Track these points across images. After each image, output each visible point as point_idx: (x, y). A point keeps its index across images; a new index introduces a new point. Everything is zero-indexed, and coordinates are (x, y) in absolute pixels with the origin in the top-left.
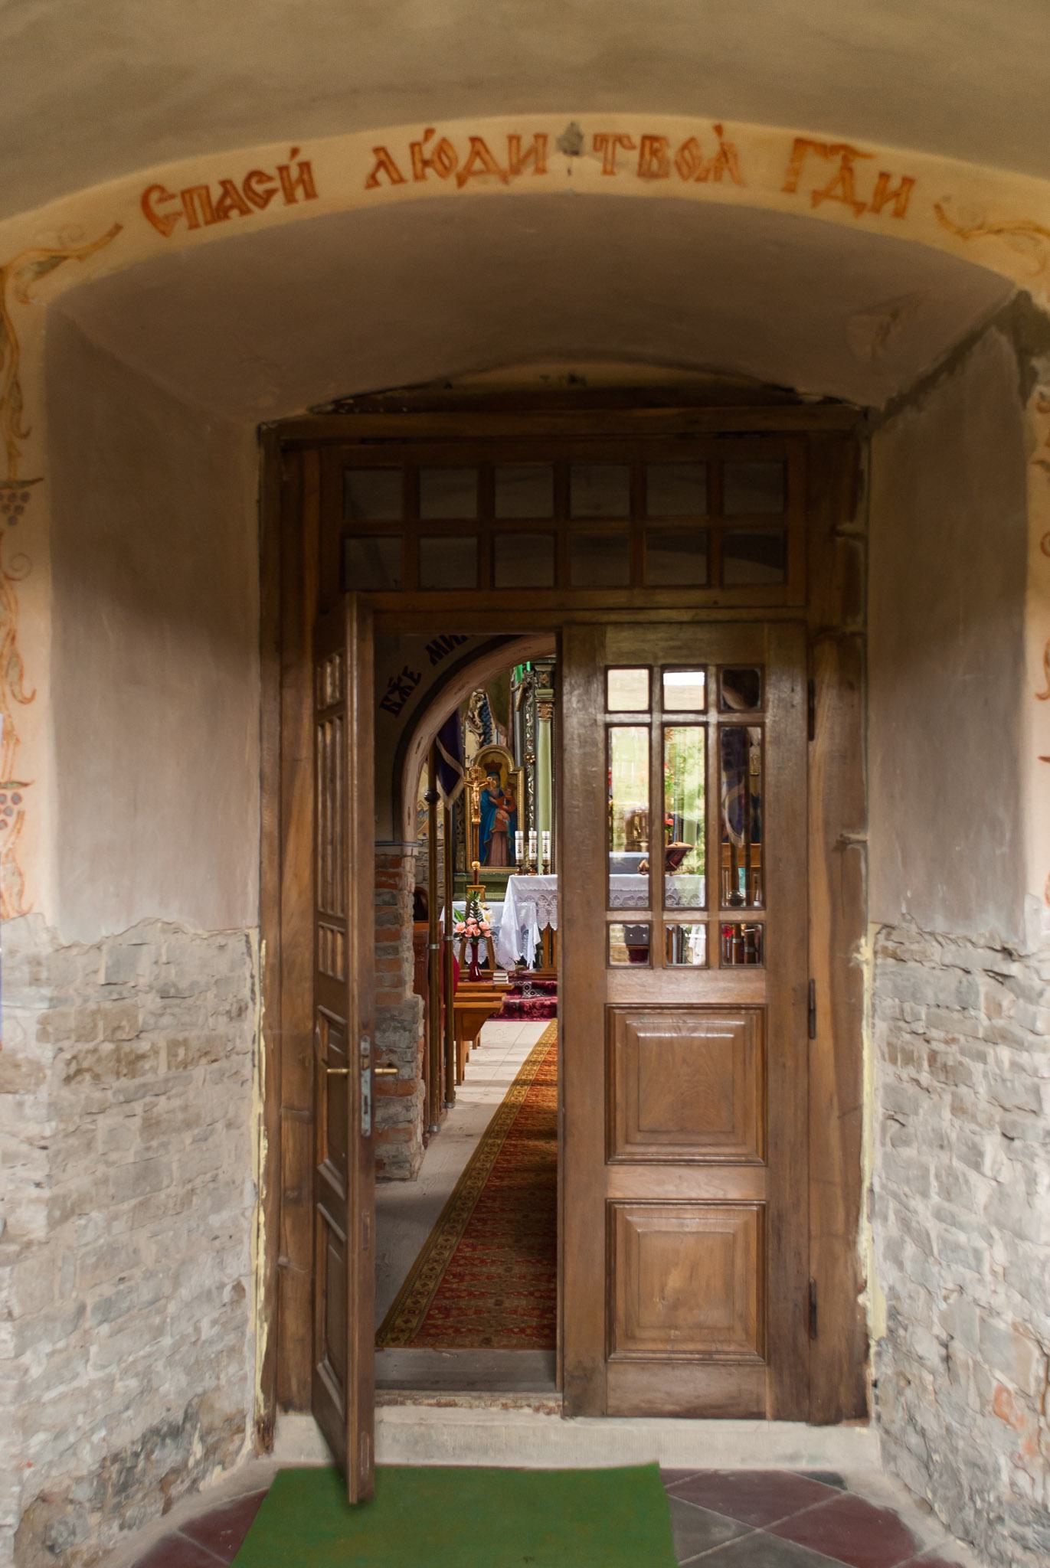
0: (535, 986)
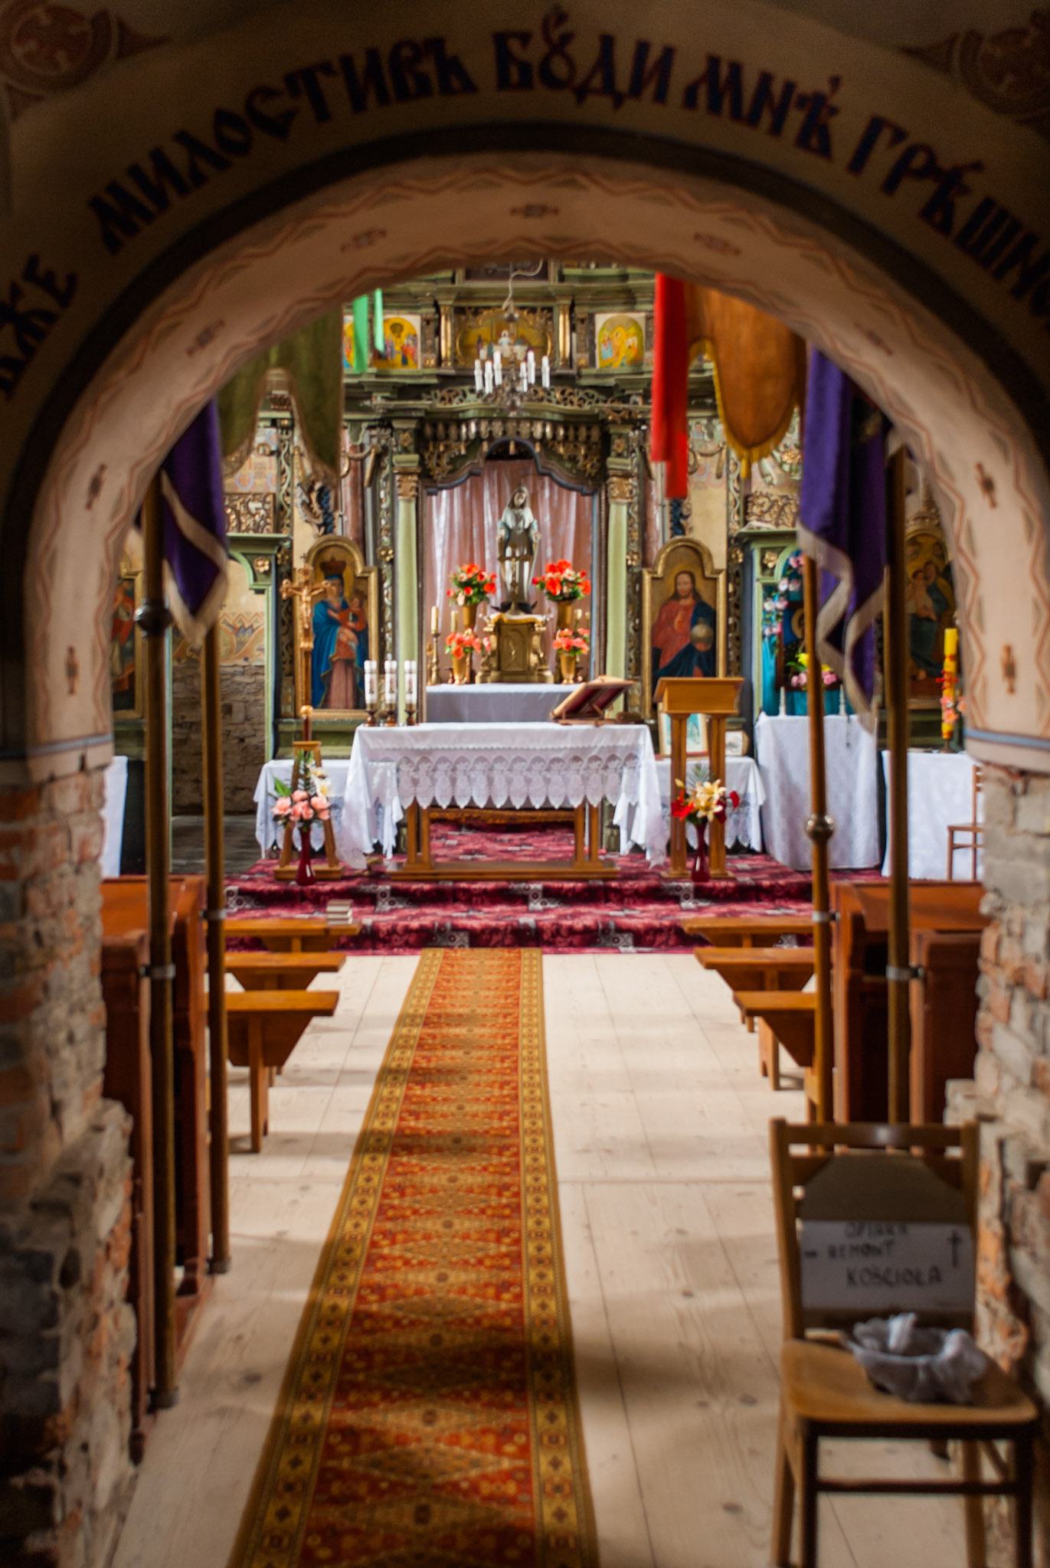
0: (396, 894)
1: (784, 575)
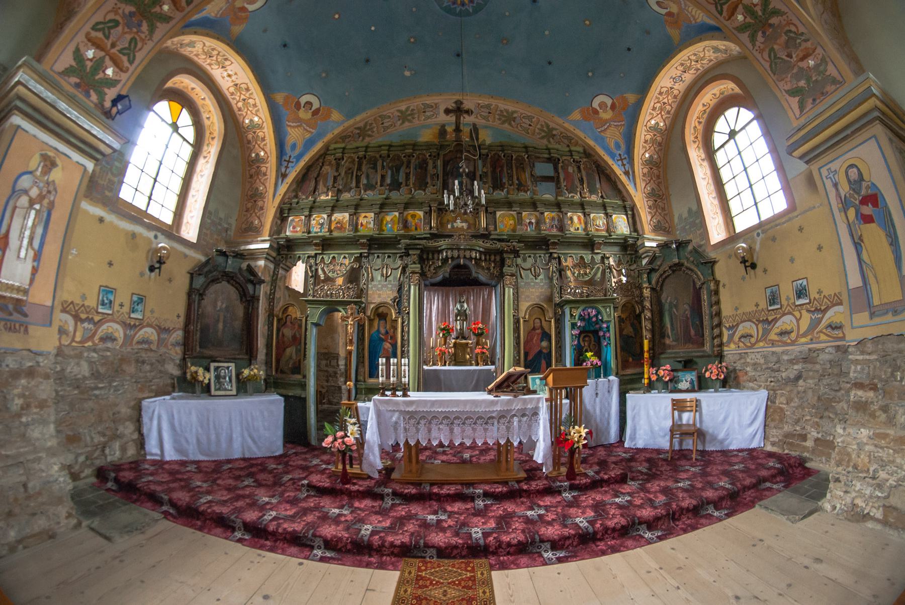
1: (579, 319)
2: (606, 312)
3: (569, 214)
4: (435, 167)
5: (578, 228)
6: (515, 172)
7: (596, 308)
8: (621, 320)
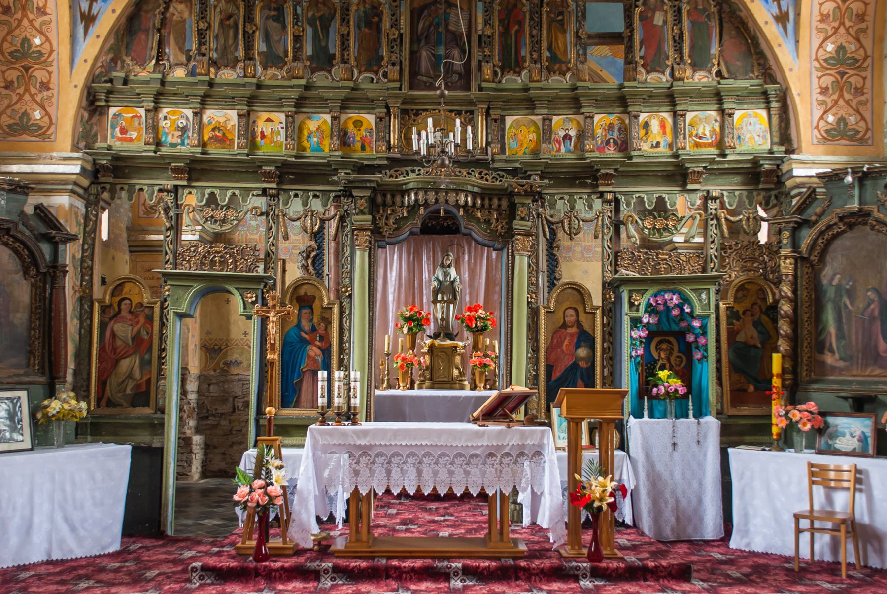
1: (646, 311)
2: (700, 300)
3: (643, 117)
4: (395, 24)
5: (658, 144)
6: (545, 33)
7: (680, 293)
8: (733, 314)
